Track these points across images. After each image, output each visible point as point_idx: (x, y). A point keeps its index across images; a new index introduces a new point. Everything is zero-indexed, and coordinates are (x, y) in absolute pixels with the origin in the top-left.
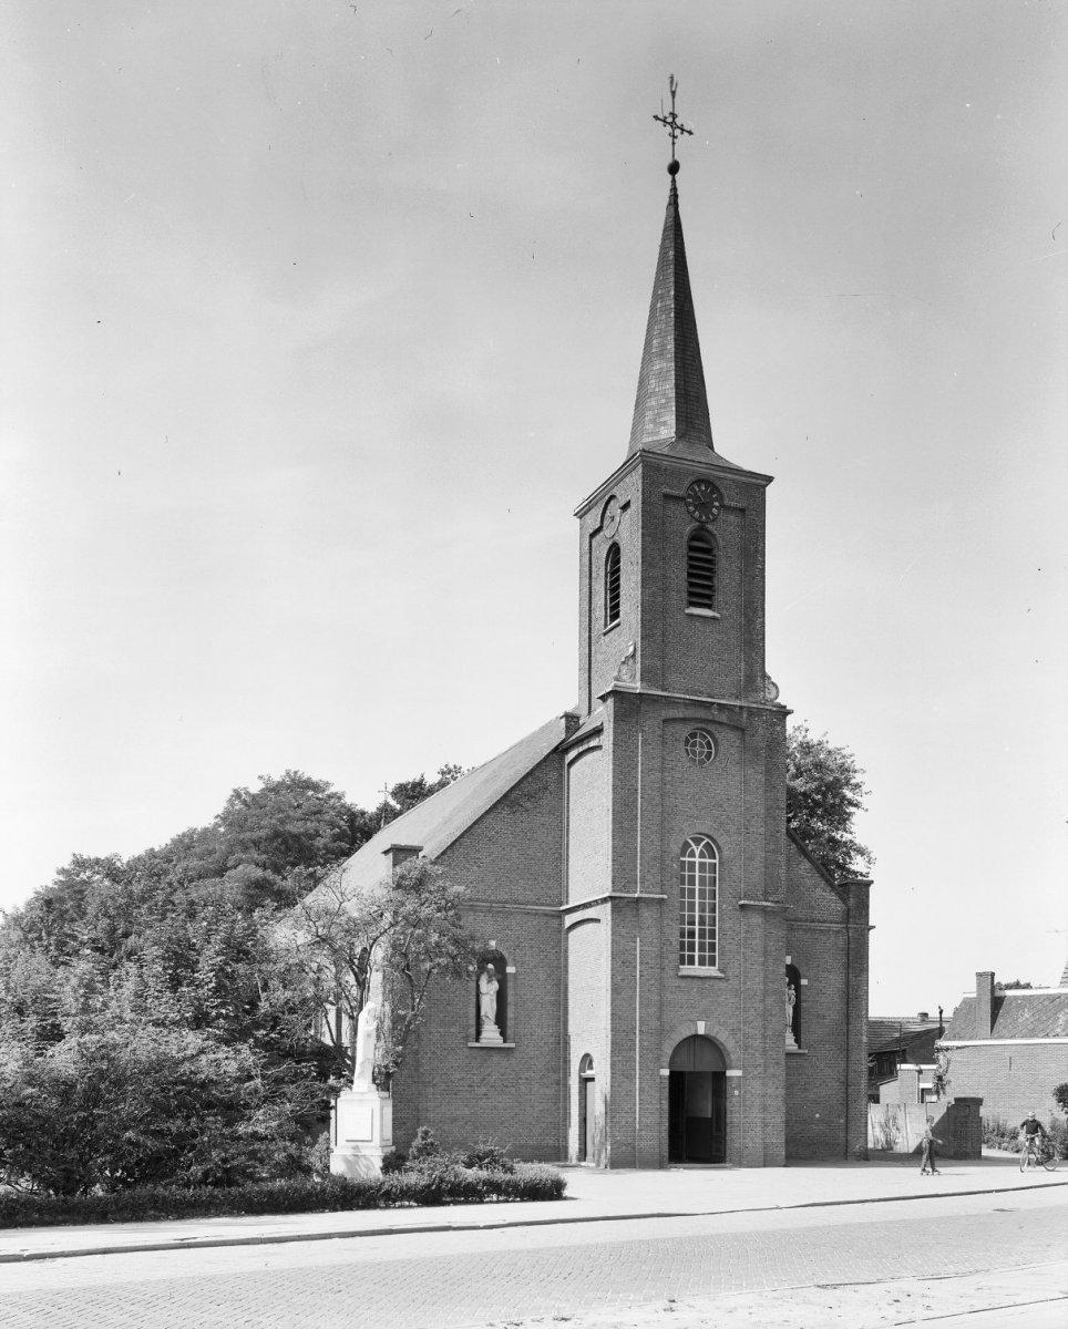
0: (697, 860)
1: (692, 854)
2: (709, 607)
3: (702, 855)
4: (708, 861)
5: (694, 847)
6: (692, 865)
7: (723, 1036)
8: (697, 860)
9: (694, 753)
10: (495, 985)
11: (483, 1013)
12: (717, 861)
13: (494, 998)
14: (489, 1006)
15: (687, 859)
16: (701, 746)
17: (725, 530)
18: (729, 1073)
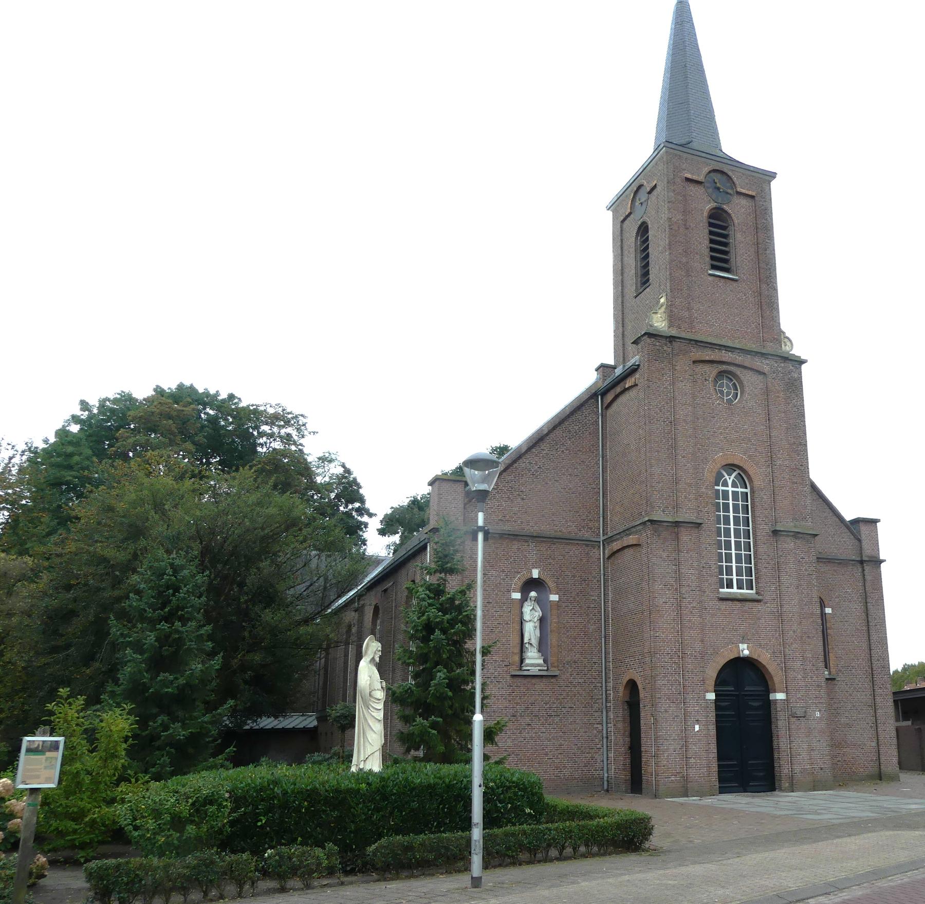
0: (730, 489)
1: (725, 484)
2: (727, 270)
3: (734, 485)
4: (740, 490)
5: (727, 477)
6: (725, 493)
7: (765, 658)
8: (730, 489)
9: (722, 392)
10: (538, 613)
11: (526, 640)
12: (748, 490)
13: (538, 624)
14: (531, 631)
15: (721, 488)
16: (728, 387)
17: (738, 210)
18: (772, 696)
